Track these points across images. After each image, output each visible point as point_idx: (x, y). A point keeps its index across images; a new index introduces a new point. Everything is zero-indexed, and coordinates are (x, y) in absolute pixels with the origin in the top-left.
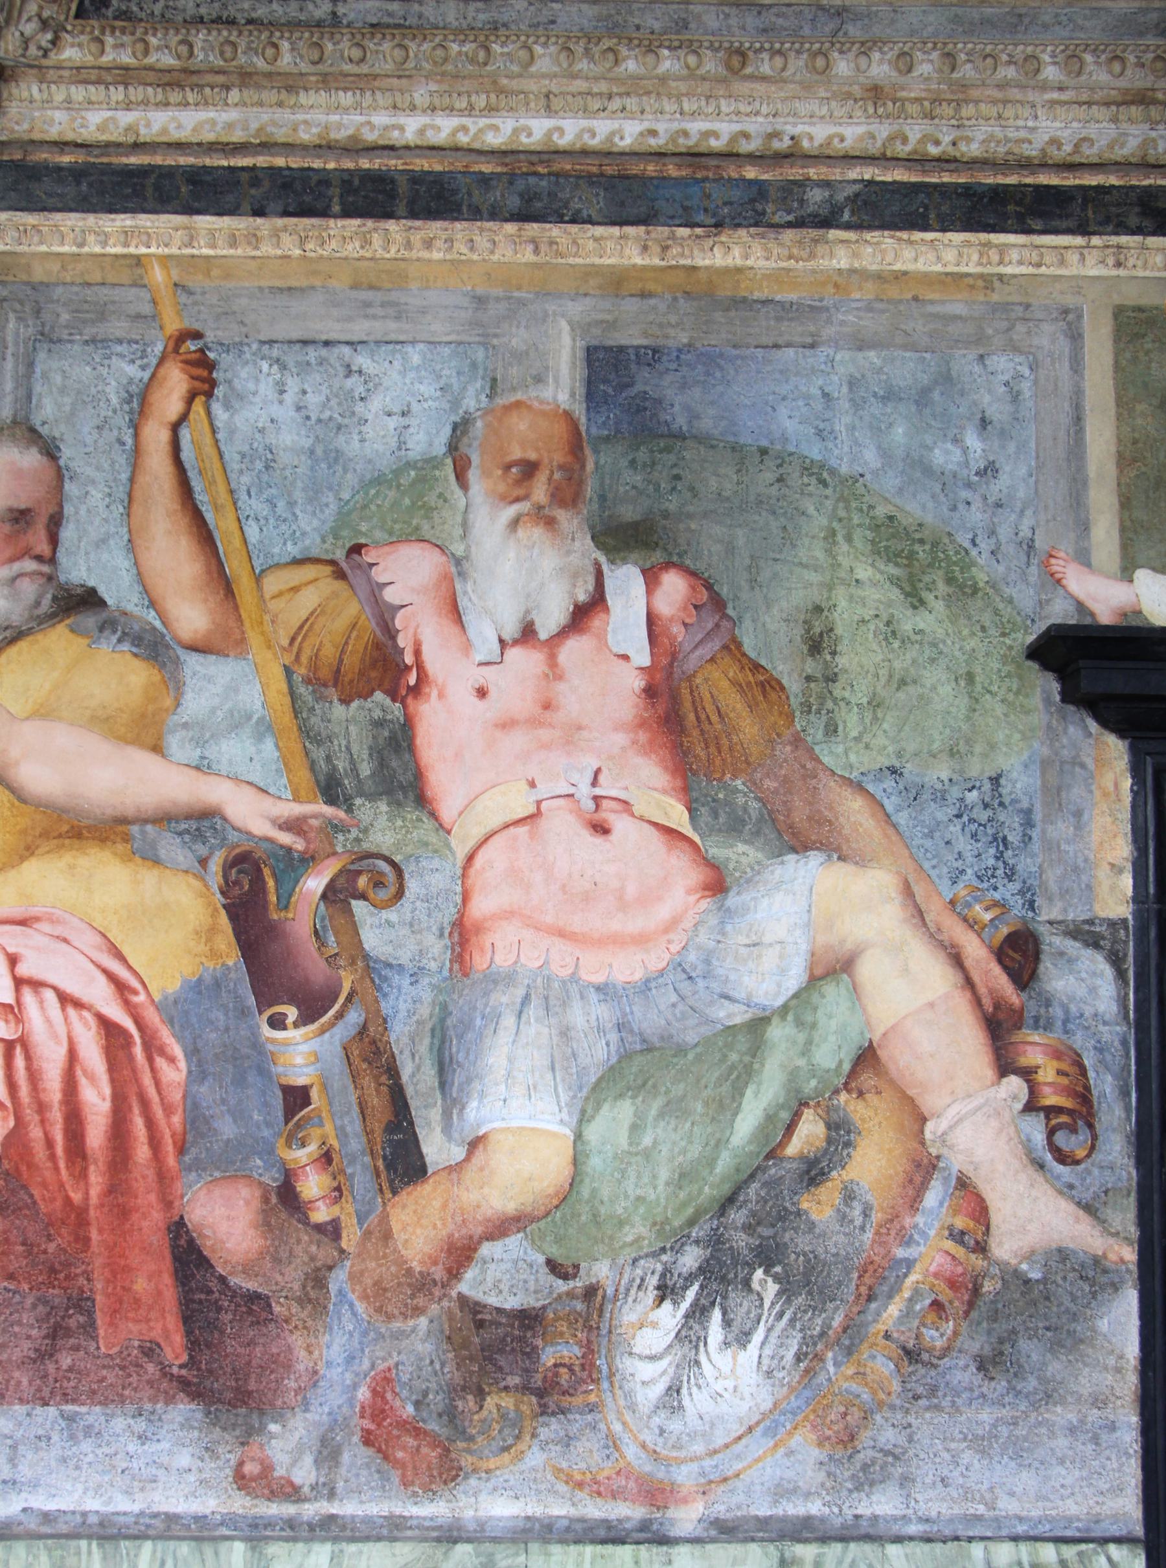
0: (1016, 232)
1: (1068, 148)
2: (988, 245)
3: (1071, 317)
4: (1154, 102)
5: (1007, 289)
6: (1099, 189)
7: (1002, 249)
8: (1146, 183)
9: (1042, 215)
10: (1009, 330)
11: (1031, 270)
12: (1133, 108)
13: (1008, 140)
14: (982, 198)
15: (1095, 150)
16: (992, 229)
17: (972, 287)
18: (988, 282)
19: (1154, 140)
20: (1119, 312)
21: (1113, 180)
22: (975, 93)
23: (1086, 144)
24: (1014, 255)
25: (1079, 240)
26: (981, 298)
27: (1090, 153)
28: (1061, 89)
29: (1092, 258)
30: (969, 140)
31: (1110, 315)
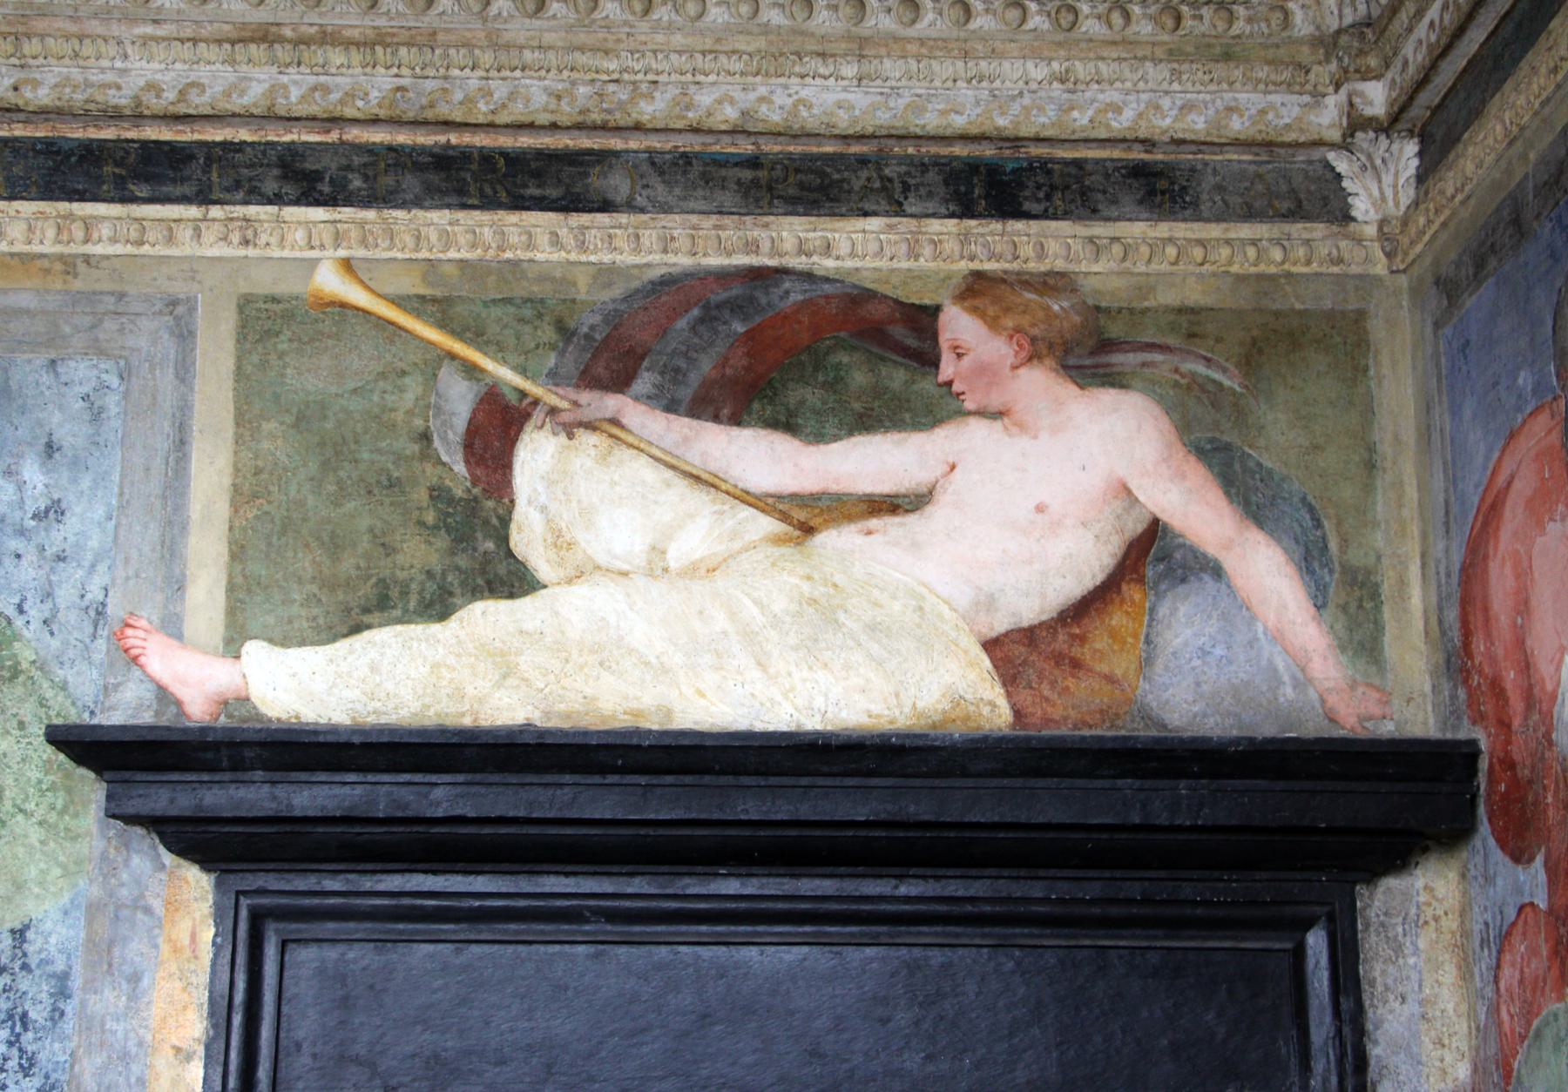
0: (111, 200)
1: (171, 95)
2: (70, 216)
3: (180, 310)
4: (281, 40)
5: (95, 273)
6: (226, 145)
7: (88, 224)
8: (287, 138)
9: (148, 179)
10: (93, 327)
11: (130, 249)
12: (253, 47)
13: (88, 84)
14: (68, 157)
15: (206, 98)
16: (82, 197)
17: (47, 271)
18: (69, 265)
19: (285, 87)
20: (245, 303)
21: (244, 135)
22: (40, 25)
23: (194, 91)
24: (106, 231)
25: (193, 211)
26: (59, 286)
27: (199, 102)
28: (155, 22)
29: (209, 235)
30: (36, 84)
31: (233, 307)
